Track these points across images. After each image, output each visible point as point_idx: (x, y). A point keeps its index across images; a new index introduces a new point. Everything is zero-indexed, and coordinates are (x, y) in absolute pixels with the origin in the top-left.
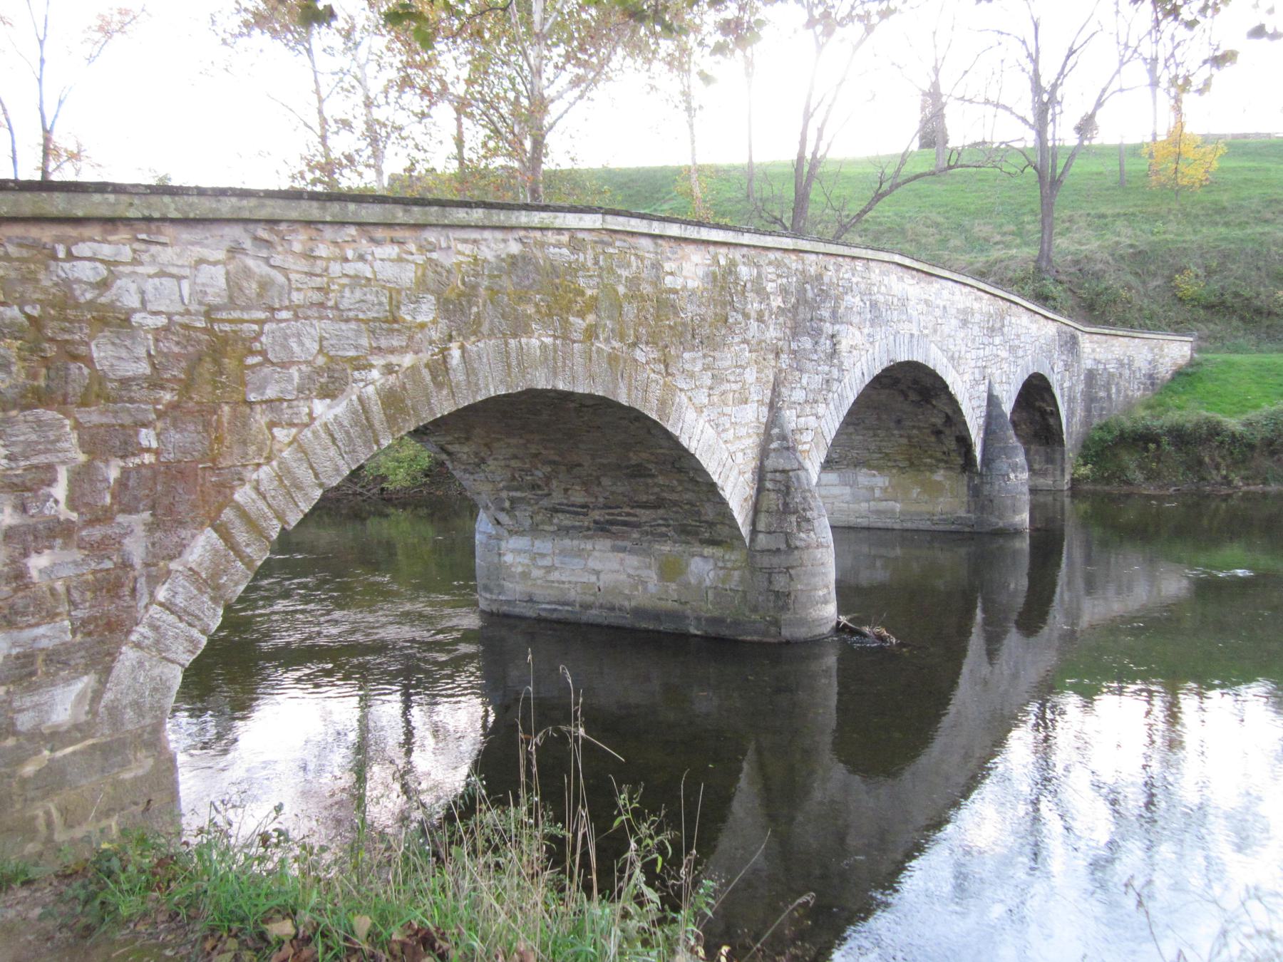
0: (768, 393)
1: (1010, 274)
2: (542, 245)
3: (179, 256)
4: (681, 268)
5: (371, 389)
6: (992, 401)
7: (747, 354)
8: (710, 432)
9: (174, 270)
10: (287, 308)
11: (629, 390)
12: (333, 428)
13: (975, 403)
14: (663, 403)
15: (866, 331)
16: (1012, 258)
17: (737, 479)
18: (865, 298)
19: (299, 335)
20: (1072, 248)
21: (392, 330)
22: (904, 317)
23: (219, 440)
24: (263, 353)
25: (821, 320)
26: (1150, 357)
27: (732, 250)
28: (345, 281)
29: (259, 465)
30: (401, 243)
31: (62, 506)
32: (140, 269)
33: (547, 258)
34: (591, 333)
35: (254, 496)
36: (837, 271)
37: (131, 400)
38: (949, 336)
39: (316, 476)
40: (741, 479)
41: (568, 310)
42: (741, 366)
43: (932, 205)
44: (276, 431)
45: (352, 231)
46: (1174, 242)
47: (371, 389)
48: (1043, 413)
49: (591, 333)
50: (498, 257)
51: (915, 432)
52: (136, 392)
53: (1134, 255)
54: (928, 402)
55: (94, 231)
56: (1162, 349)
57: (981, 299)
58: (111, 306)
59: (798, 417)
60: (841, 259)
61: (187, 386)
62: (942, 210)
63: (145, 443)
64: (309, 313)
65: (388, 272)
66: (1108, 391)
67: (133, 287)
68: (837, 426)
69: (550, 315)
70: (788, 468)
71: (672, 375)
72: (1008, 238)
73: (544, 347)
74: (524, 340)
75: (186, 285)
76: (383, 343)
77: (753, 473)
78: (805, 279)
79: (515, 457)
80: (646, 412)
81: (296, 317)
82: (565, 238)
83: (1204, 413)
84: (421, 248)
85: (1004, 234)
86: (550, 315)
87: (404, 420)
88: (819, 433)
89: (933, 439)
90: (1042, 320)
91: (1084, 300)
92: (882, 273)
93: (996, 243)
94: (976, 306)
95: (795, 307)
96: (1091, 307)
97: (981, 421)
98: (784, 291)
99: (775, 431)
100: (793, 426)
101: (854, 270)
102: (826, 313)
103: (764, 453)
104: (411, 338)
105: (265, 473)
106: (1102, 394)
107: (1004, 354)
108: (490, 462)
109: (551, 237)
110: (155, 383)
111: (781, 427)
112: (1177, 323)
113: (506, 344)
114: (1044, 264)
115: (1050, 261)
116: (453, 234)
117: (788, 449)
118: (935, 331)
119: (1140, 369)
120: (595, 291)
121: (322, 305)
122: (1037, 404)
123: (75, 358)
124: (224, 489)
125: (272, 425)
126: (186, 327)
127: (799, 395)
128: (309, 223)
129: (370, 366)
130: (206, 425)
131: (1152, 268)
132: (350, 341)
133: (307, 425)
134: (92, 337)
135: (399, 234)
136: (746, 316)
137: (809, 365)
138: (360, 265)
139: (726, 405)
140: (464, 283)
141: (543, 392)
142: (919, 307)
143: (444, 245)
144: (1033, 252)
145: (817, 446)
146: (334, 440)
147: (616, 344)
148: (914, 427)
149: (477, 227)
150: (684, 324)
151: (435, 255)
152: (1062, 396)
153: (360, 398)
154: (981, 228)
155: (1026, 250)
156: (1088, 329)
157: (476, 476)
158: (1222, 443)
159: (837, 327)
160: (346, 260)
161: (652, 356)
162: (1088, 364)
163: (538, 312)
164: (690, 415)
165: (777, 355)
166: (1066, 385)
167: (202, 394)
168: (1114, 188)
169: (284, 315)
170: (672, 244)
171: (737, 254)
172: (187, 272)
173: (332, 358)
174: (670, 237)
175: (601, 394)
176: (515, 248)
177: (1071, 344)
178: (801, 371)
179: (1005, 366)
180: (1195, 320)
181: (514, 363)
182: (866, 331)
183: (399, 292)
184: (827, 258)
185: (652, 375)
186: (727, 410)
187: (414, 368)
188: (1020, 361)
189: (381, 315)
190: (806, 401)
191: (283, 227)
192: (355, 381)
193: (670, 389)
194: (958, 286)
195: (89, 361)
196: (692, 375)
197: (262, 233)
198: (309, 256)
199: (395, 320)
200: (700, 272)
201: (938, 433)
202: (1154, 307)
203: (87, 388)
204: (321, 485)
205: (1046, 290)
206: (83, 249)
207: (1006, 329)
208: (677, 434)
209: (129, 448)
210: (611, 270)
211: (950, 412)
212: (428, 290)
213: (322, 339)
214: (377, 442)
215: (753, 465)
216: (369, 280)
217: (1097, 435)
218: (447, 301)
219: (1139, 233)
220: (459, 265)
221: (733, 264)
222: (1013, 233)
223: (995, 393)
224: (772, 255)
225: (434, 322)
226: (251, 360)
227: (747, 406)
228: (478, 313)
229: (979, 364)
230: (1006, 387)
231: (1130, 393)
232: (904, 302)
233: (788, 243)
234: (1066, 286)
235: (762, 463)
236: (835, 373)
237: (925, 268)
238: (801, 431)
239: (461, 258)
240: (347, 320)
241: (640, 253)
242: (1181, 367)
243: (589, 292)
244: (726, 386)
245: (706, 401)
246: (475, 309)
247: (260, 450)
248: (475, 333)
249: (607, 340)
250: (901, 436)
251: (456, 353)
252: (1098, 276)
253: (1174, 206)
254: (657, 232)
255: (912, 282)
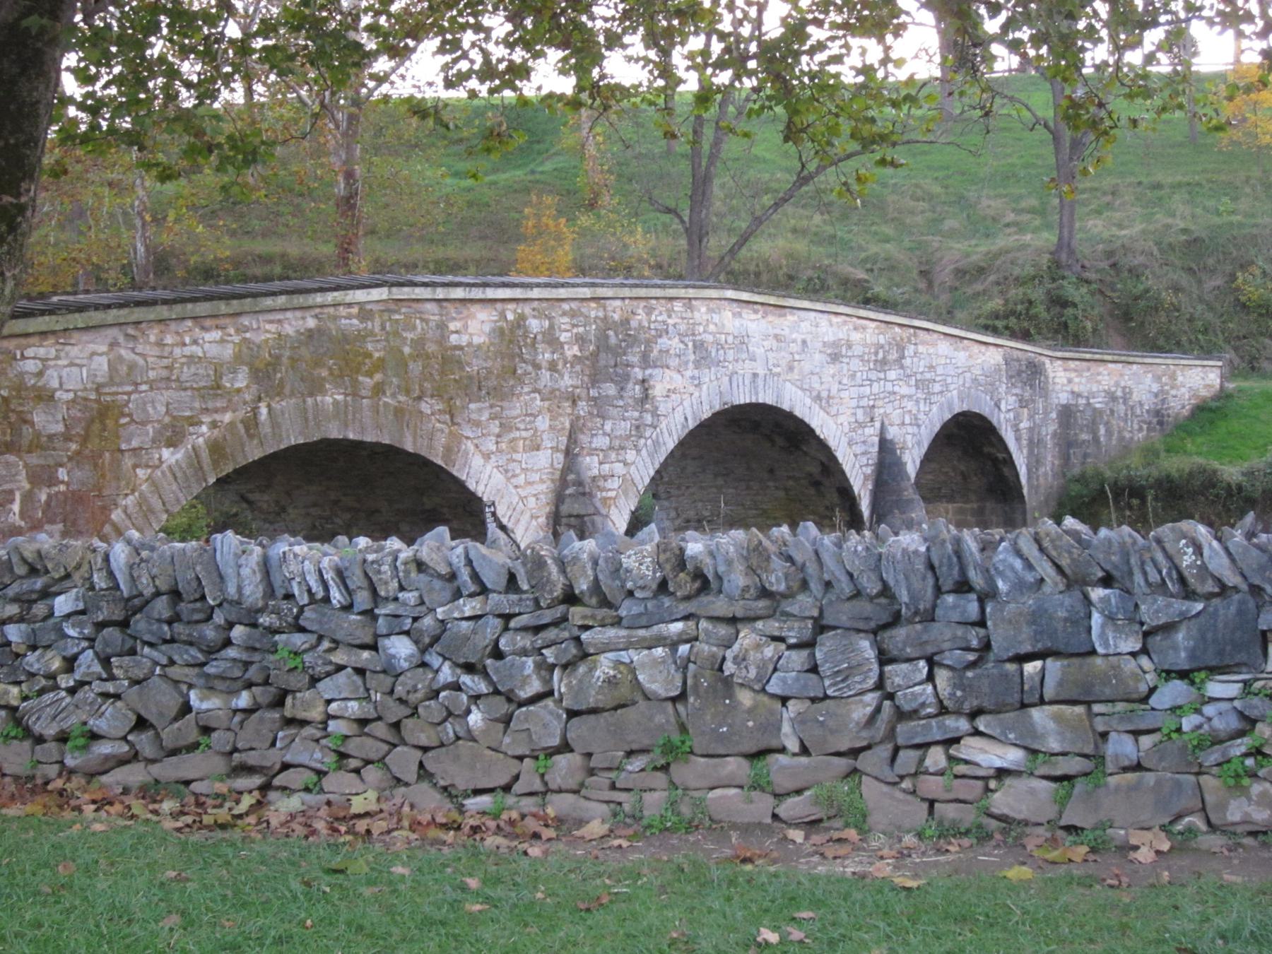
0: (564, 440)
1: (1017, 271)
2: (335, 318)
3: (81, 351)
4: (466, 327)
5: (201, 440)
6: (886, 446)
7: (538, 402)
8: (498, 477)
9: (78, 361)
10: (146, 383)
11: (415, 438)
12: (176, 469)
13: (859, 449)
14: (448, 450)
15: (688, 373)
16: (1024, 247)
17: (529, 523)
18: (686, 339)
19: (153, 402)
20: (1106, 235)
21: (217, 395)
22: (744, 356)
23: (103, 476)
24: (130, 415)
25: (628, 365)
26: (1155, 387)
27: (521, 305)
28: (184, 360)
29: (127, 495)
30: (223, 328)
31: (17, 517)
32: (60, 362)
33: (339, 328)
34: (379, 390)
35: (123, 516)
36: (649, 314)
37: (54, 449)
38: (812, 373)
39: (164, 504)
40: (534, 523)
41: (358, 371)
42: (531, 415)
43: (929, 168)
44: (138, 471)
45: (189, 323)
46: (1241, 225)
47: (201, 440)
48: (995, 461)
49: (379, 390)
50: (297, 331)
51: (791, 483)
52: (57, 444)
53: (1189, 244)
54: (798, 448)
55: (34, 340)
56: (1173, 377)
57: (864, 328)
58: (43, 388)
59: (601, 463)
60: (654, 302)
61: (85, 439)
62: (940, 174)
63: (61, 477)
64: (160, 385)
65: (213, 350)
66: (1095, 434)
67: (55, 374)
68: (652, 473)
69: (341, 376)
70: (583, 512)
71: (458, 424)
72: (1025, 217)
73: (336, 403)
74: (319, 398)
75: (84, 371)
76: (210, 405)
77: (547, 518)
78: (606, 323)
79: (315, 505)
80: (432, 458)
81: (151, 389)
82: (355, 310)
83: (1200, 460)
84: (238, 331)
85: (1022, 211)
86: (341, 376)
87: (225, 464)
88: (627, 481)
89: (812, 491)
90: (976, 348)
91: (1117, 306)
92: (710, 311)
93: (1008, 225)
94: (856, 337)
95: (595, 356)
96: (1127, 317)
97: (869, 470)
98: (581, 340)
99: (571, 477)
100: (595, 472)
101: (670, 313)
102: (635, 359)
103: (559, 499)
104: (230, 401)
105: (130, 501)
106: (1084, 436)
107: (905, 390)
108: (290, 510)
109: (343, 311)
110: (67, 438)
111: (578, 474)
112: (1238, 338)
113: (304, 402)
114: (1064, 257)
115: (1071, 252)
116: (261, 317)
117: (584, 494)
118: (791, 369)
119: (1141, 404)
120: (382, 354)
121: (168, 379)
122: (986, 450)
123: (25, 422)
124: (106, 510)
125: (135, 466)
126: (86, 399)
127: (601, 442)
128: (160, 321)
129: (200, 423)
130: (96, 465)
131: (1211, 261)
132: (187, 403)
133: (158, 467)
134: (34, 408)
135: (222, 321)
136: (537, 367)
137: (613, 412)
138: (194, 348)
139: (516, 452)
140: (270, 355)
141: (336, 441)
142: (765, 343)
143: (255, 326)
144: (1049, 238)
145: (626, 493)
146: (175, 478)
147: (402, 398)
148: (789, 478)
149: (281, 310)
150: (470, 378)
151: (248, 335)
152: (1018, 439)
153: (194, 448)
154: (990, 204)
155: (1045, 235)
156: (1059, 354)
157: (276, 526)
158: (1217, 496)
159: (648, 372)
160: (184, 345)
161: (437, 407)
162: (1064, 398)
163: (331, 374)
164: (477, 461)
165: (574, 402)
166: (1024, 425)
167: (94, 444)
168: (1181, 145)
169: (144, 387)
170: (458, 305)
171: (527, 309)
172: (85, 362)
173: (174, 418)
174: (455, 300)
175: (387, 442)
176: (311, 323)
177: (1032, 374)
178: (604, 418)
179: (910, 405)
180: (1262, 334)
181: (311, 417)
182: (688, 373)
183: (222, 365)
184: (635, 303)
185: (438, 425)
186: (515, 456)
187: (232, 424)
188: (934, 398)
189: (209, 384)
190: (611, 448)
191: (144, 325)
192: (191, 434)
193: (456, 439)
194: (825, 316)
195: (32, 424)
196: (478, 424)
197: (131, 331)
198: (160, 344)
199: (219, 387)
200: (487, 328)
201: (817, 484)
202: (1209, 316)
203: (31, 441)
204: (167, 511)
205: (1061, 292)
206: (30, 352)
207: (907, 362)
208: (464, 478)
209: (53, 481)
210: (397, 334)
211: (824, 459)
212: (243, 363)
213: (168, 404)
214: (205, 480)
215: (548, 509)
216: (200, 358)
217: (1076, 488)
218: (257, 370)
219: (1199, 211)
220: (267, 341)
221: (522, 318)
222: (1032, 211)
223: (889, 437)
224: (566, 306)
225: (247, 387)
226: (124, 421)
227: (540, 453)
228: (281, 378)
229: (864, 402)
230: (910, 429)
231: (1127, 435)
232: (742, 341)
233: (586, 292)
234: (1094, 286)
235: (557, 507)
236: (648, 418)
237: (772, 300)
238: (605, 478)
239: (268, 336)
240: (185, 389)
241: (426, 316)
242: (1204, 400)
243: (377, 355)
244: (517, 434)
245: (494, 448)
246: (279, 375)
247: (128, 484)
248: (278, 394)
249: (393, 395)
250: (777, 488)
251: (264, 411)
252: (1135, 273)
253: (1256, 172)
254: (441, 297)
255: (753, 316)
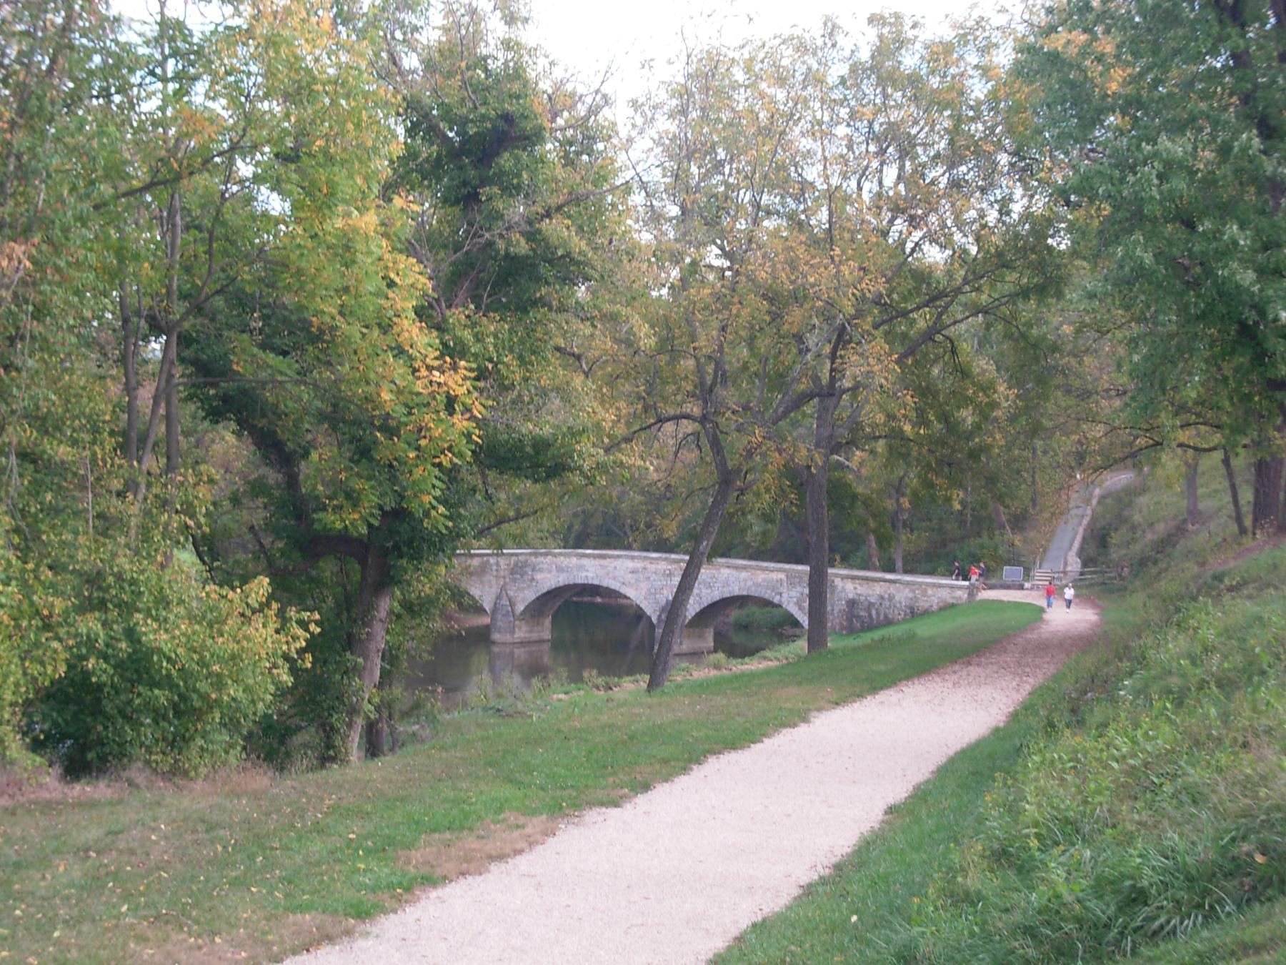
26: (911, 595)
94: (649, 566)
106: (862, 613)
162: (851, 596)
